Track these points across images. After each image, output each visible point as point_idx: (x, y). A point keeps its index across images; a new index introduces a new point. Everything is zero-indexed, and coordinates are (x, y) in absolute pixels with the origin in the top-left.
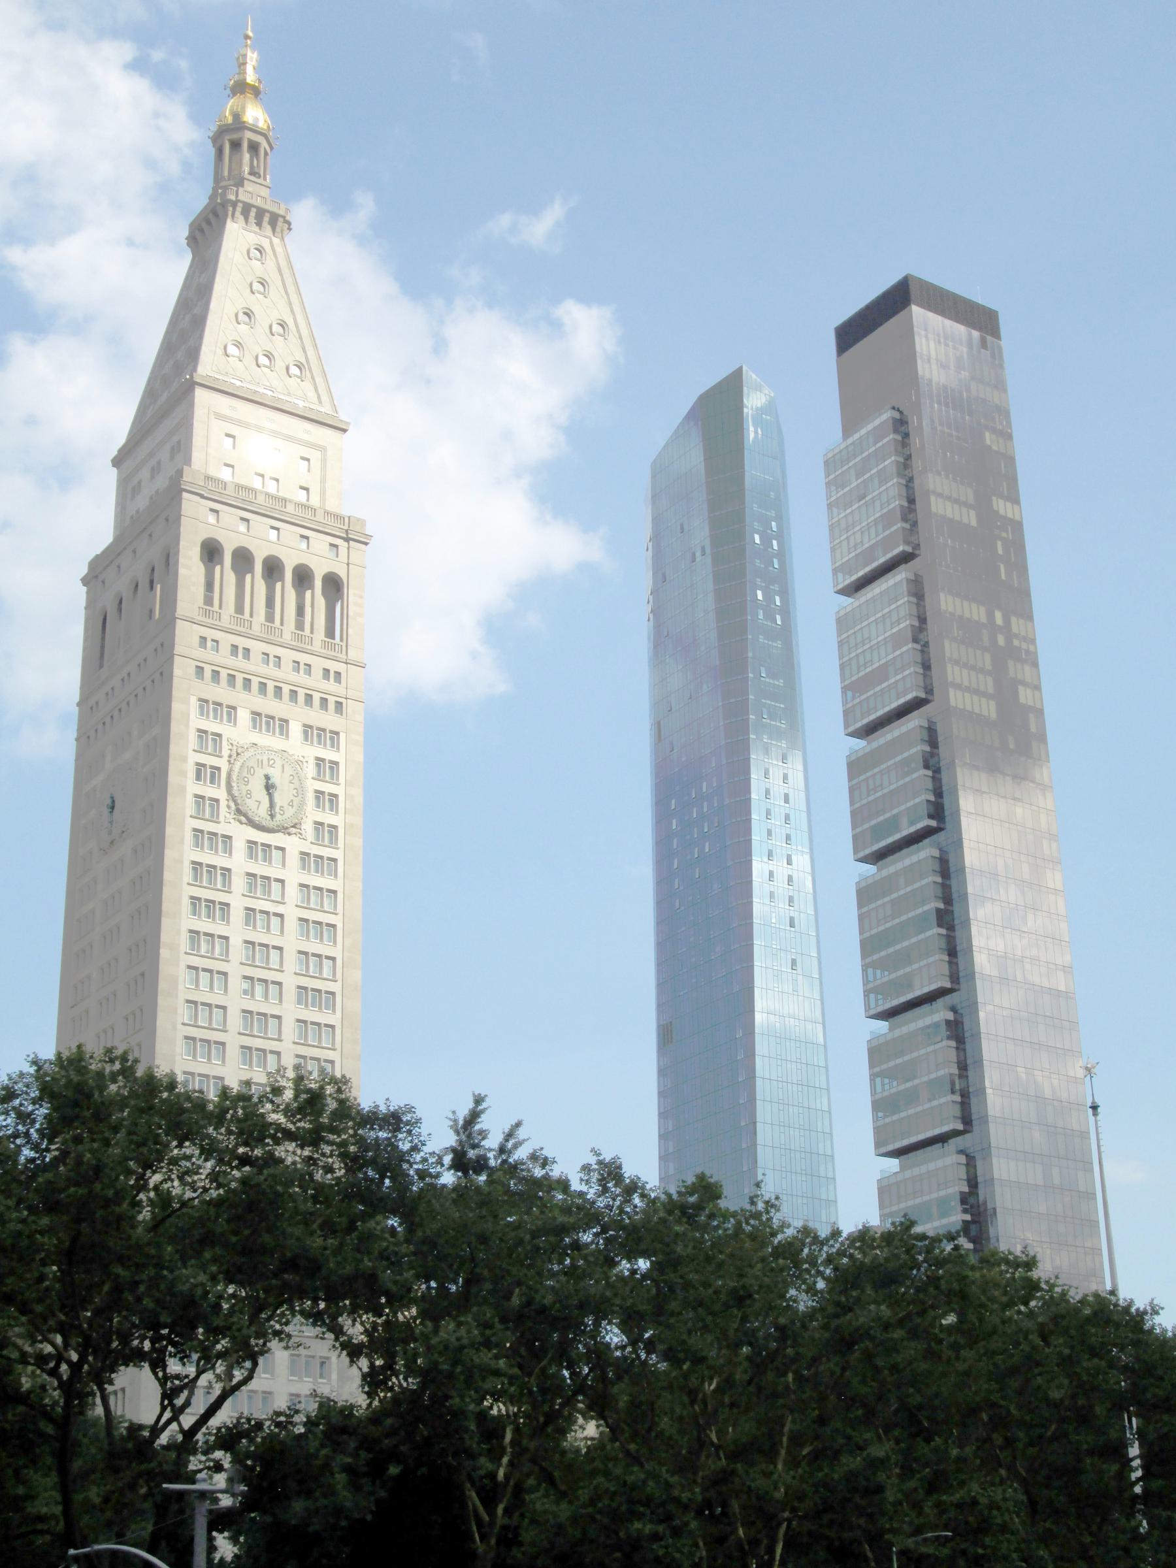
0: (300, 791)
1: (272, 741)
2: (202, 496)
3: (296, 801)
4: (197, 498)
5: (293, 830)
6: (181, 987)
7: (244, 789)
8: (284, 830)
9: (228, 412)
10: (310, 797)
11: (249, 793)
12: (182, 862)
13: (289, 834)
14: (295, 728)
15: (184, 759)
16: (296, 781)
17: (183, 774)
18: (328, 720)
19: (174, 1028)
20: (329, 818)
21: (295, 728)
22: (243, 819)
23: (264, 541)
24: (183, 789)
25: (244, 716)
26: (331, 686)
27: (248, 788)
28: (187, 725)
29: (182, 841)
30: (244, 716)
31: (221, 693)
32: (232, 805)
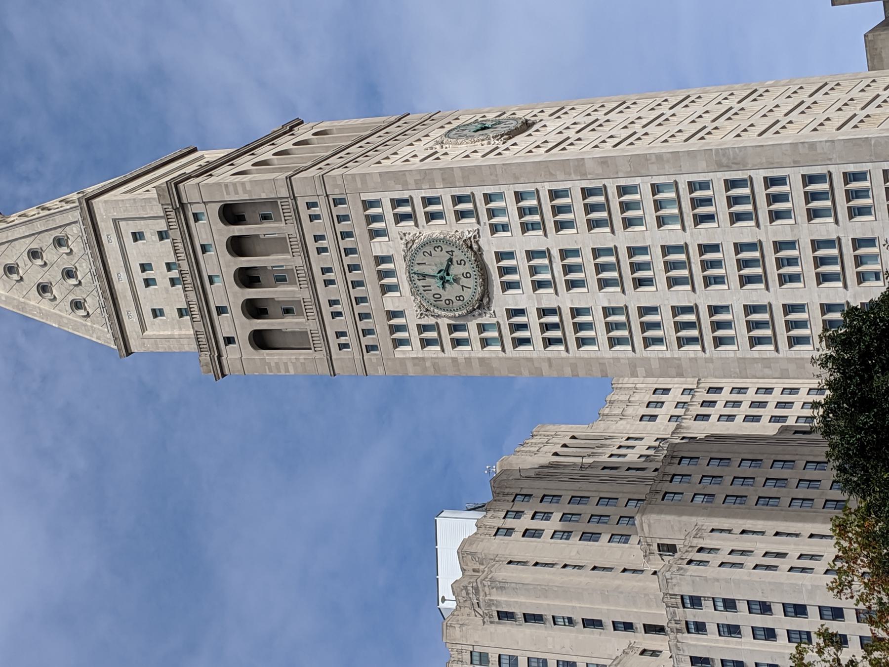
0: (435, 243)
1: (400, 266)
2: (220, 356)
3: (446, 248)
4: (224, 358)
5: (475, 247)
6: (668, 354)
7: (457, 304)
8: (478, 255)
9: (135, 319)
10: (436, 229)
11: (459, 298)
12: (549, 359)
13: (480, 249)
14: (380, 246)
15: (454, 360)
16: (428, 249)
17: (468, 360)
19: (710, 360)
20: (447, 206)
21: (380, 246)
22: (485, 301)
23: (227, 293)
24: (482, 360)
25: (391, 301)
26: (321, 210)
27: (454, 299)
28: (423, 359)
29: (530, 360)
30: (391, 301)
31: (380, 324)
32: (476, 313)
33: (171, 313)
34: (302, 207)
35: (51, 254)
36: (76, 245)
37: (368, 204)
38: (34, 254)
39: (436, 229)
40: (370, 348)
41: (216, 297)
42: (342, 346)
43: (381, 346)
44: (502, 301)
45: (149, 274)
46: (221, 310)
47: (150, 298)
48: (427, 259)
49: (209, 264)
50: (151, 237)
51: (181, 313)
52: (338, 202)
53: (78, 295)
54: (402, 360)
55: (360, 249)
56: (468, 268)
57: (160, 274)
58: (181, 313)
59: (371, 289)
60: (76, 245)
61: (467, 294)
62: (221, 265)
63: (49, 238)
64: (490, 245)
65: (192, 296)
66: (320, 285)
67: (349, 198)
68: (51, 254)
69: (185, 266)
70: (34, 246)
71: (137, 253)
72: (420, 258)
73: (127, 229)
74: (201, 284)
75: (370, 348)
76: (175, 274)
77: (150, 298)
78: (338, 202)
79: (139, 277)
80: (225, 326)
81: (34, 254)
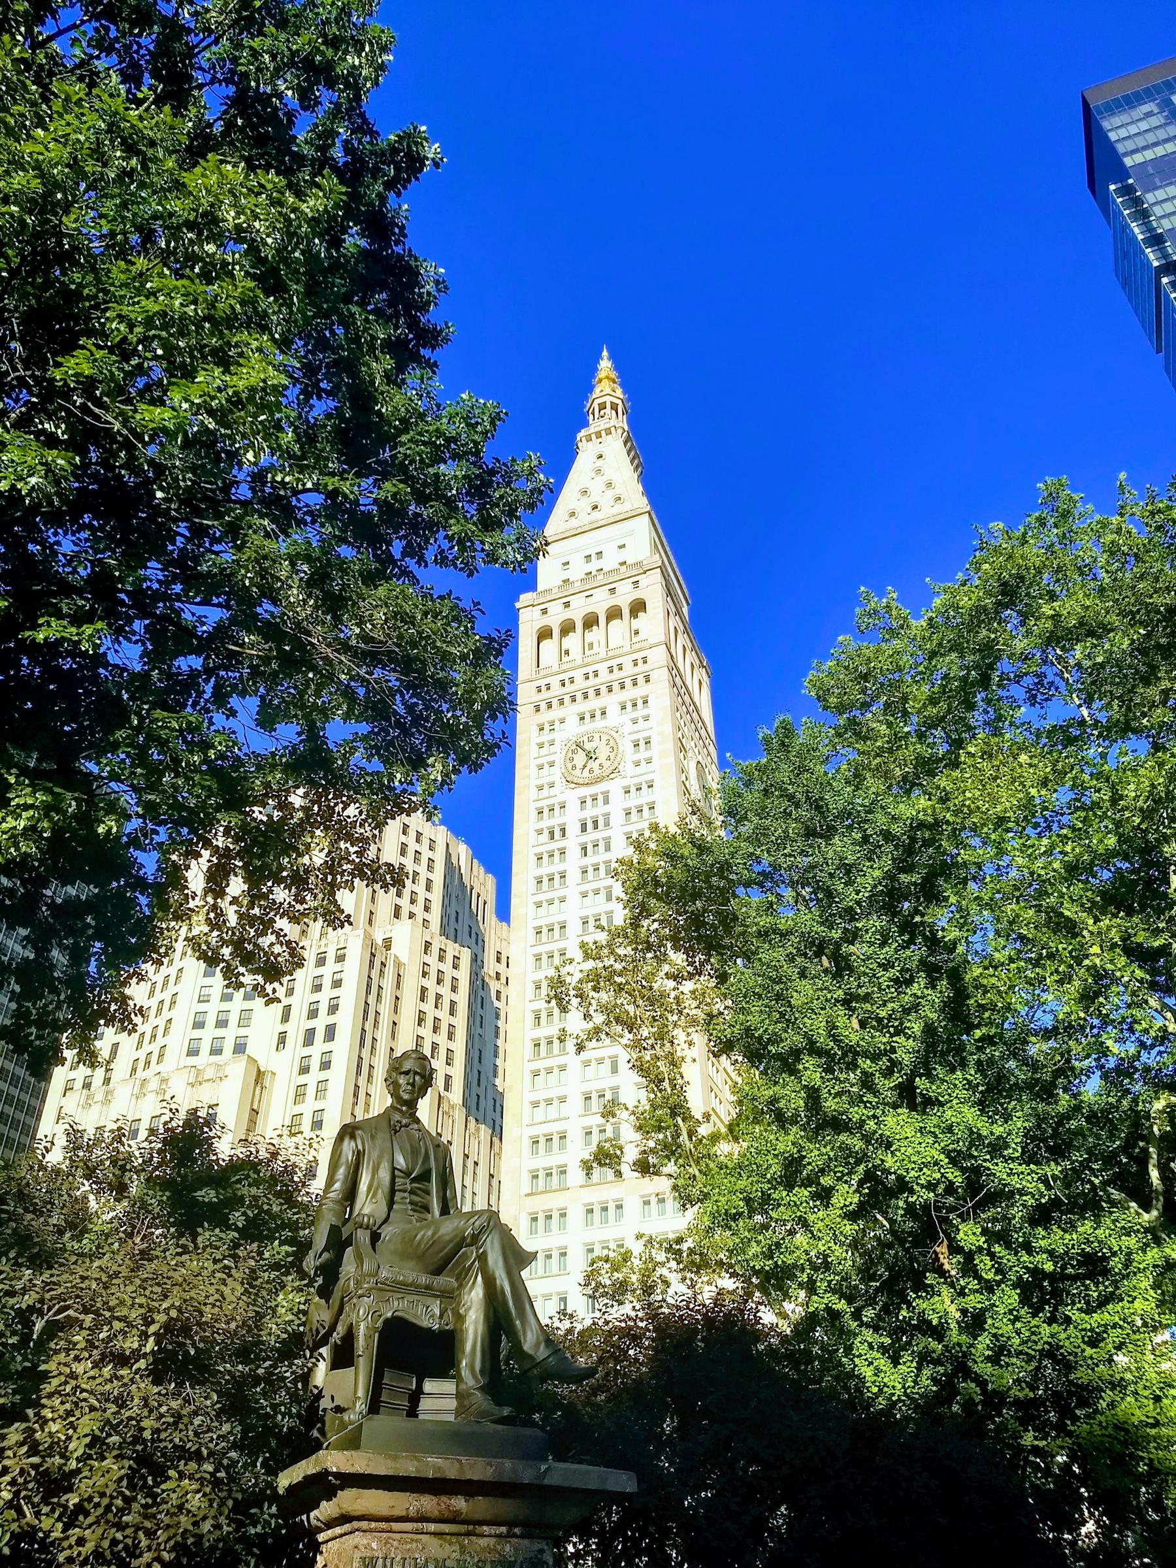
1: (599, 723)
7: (570, 766)
14: (613, 711)
34: (643, 654)
35: (611, 494)
36: (618, 508)
38: (609, 485)
39: (626, 745)
41: (576, 601)
44: (572, 797)
48: (604, 742)
55: (612, 696)
56: (597, 771)
57: (594, 566)
58: (566, 581)
59: (582, 706)
61: (577, 772)
62: (600, 603)
64: (614, 787)
68: (611, 494)
72: (605, 737)
81: (609, 485)
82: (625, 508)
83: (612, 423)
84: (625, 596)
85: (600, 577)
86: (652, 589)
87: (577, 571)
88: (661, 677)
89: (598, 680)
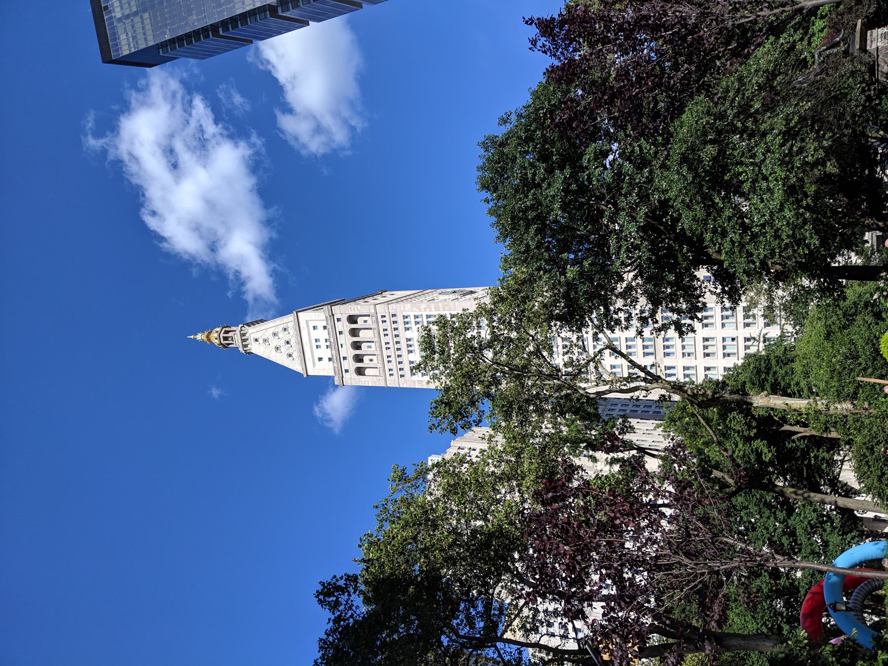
14: (408, 334)
18: (400, 319)
21: (408, 334)
23: (348, 352)
33: (325, 360)
34: (379, 317)
35: (281, 335)
36: (291, 331)
37: (405, 317)
40: (402, 376)
42: (391, 375)
43: (406, 375)
45: (318, 344)
46: (345, 358)
47: (318, 353)
49: (342, 339)
50: (320, 328)
51: (330, 359)
52: (394, 315)
53: (291, 351)
54: (414, 382)
55: (401, 335)
57: (323, 344)
58: (330, 359)
59: (404, 351)
60: (291, 331)
62: (346, 340)
63: (280, 328)
65: (334, 352)
66: (384, 349)
67: (398, 315)
69: (332, 340)
70: (275, 331)
71: (315, 334)
73: (311, 325)
74: (338, 347)
75: (402, 376)
76: (328, 344)
77: (318, 353)
78: (394, 315)
79: (314, 344)
80: (345, 365)
81: (275, 334)
82: (291, 326)
83: (238, 332)
84: (344, 326)
85: (332, 340)
86: (342, 311)
87: (326, 353)
88: (393, 308)
89: (391, 342)
